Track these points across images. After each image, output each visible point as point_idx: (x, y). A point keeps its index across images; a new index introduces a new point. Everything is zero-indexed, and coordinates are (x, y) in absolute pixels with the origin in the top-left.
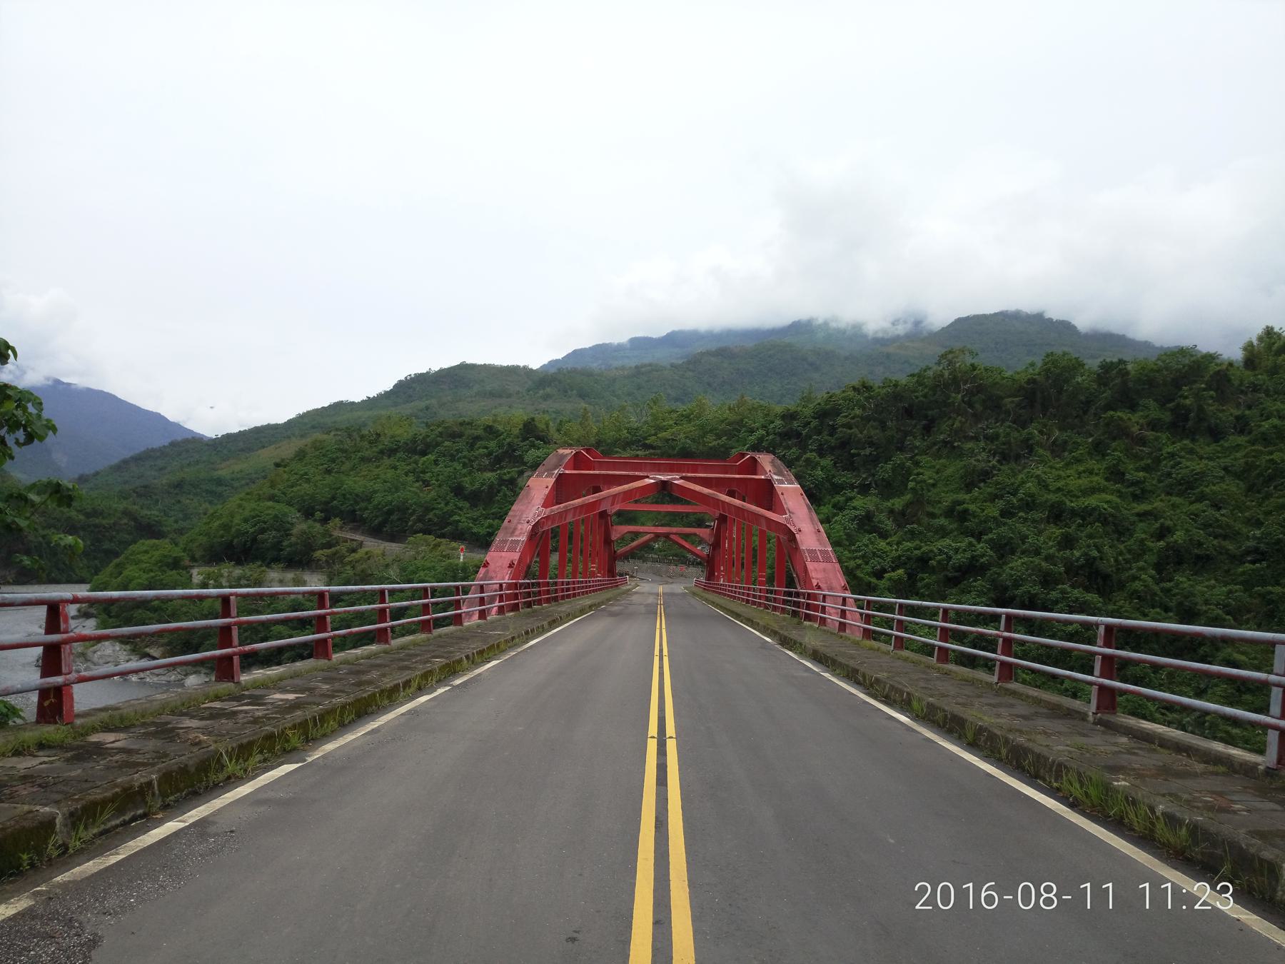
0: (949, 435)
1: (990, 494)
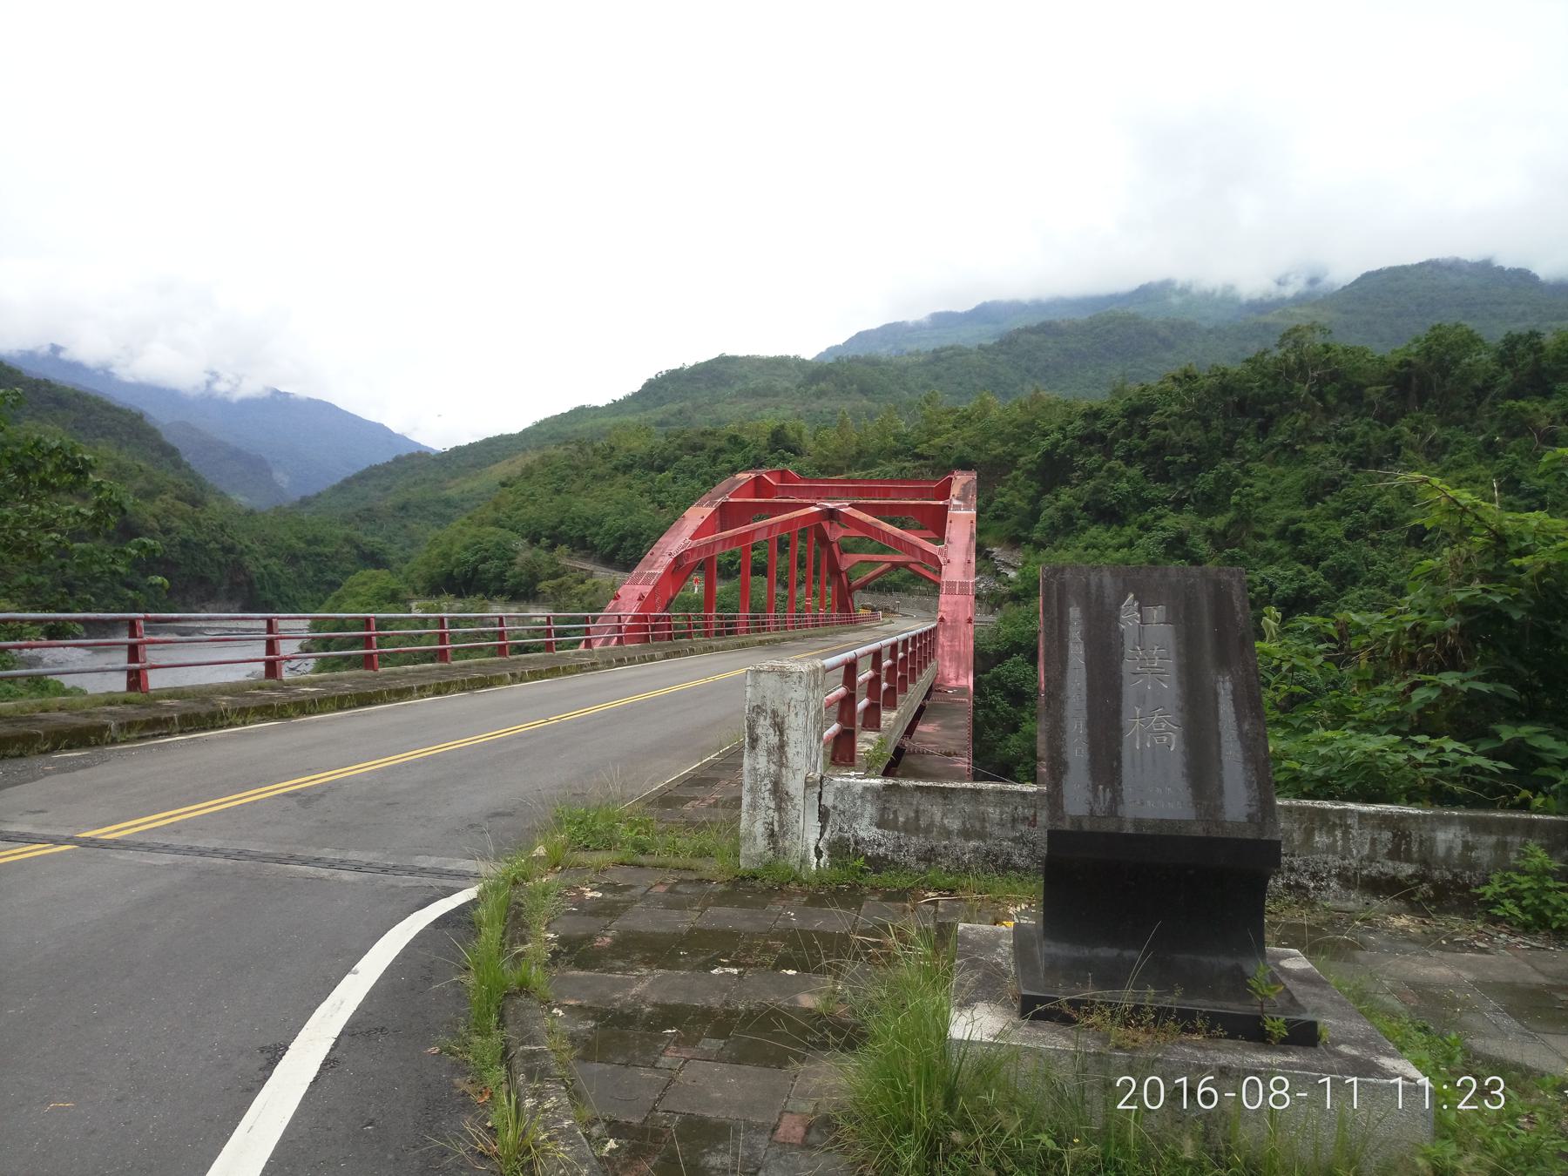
0: (1290, 436)
1: (1336, 509)
